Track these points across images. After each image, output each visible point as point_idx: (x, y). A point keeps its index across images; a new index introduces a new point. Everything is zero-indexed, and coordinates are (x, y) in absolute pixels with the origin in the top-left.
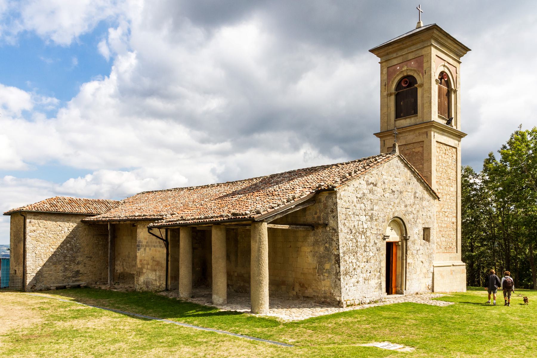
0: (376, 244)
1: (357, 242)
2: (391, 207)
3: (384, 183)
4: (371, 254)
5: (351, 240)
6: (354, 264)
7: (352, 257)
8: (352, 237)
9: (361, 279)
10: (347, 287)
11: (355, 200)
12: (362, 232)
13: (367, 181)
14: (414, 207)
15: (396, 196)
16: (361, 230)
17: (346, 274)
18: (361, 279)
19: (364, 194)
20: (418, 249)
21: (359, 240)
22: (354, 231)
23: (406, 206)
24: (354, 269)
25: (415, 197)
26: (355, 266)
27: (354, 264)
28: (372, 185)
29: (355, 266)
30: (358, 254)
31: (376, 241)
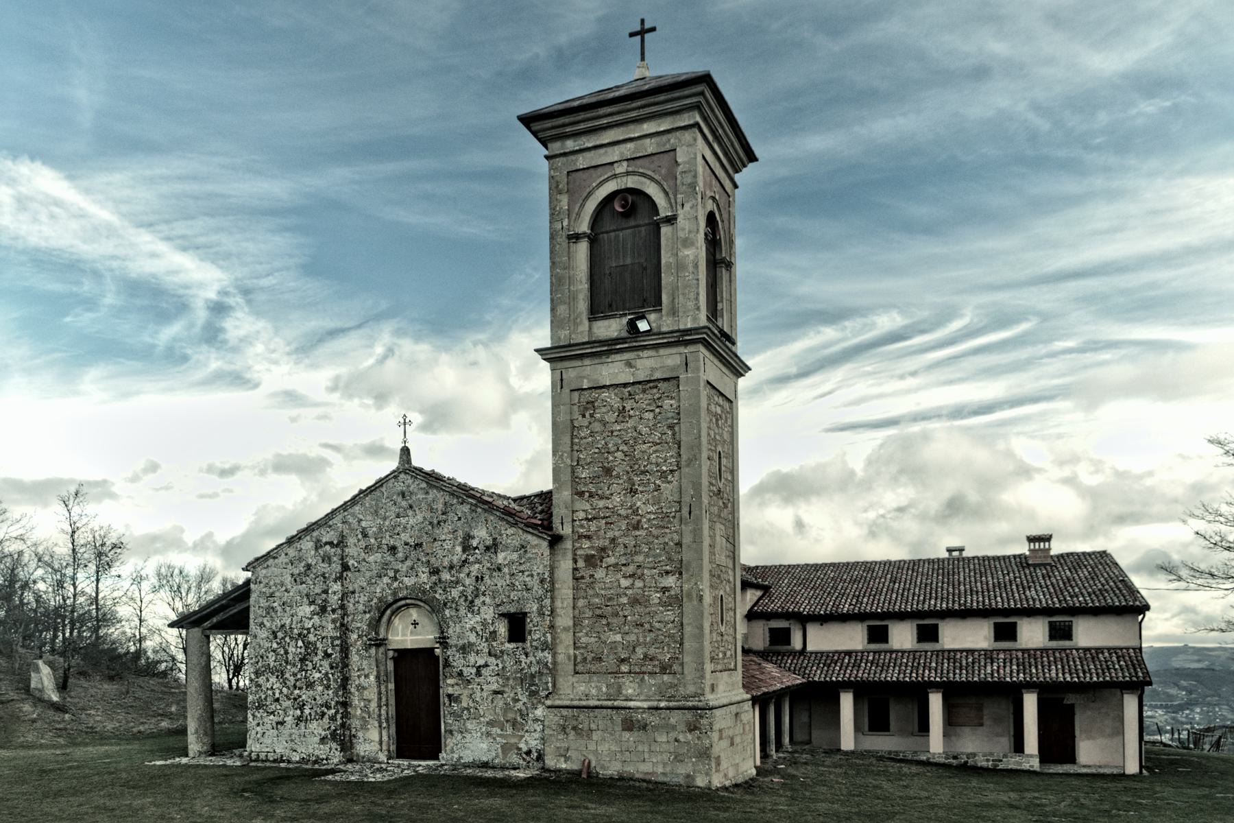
0: (327, 655)
1: (286, 653)
2: (386, 580)
3: (365, 535)
4: (317, 675)
5: (274, 651)
6: (277, 692)
7: (273, 679)
8: (275, 645)
9: (289, 719)
10: (258, 729)
11: (288, 579)
12: (299, 635)
13: (318, 541)
14: (466, 570)
15: (400, 555)
16: (296, 631)
17: (258, 708)
18: (289, 719)
19: (309, 567)
20: (481, 662)
21: (291, 649)
22: (280, 635)
23: (435, 572)
24: (277, 700)
25: (464, 551)
26: (277, 695)
27: (277, 692)
28: (328, 547)
29: (277, 695)
30: (287, 675)
31: (330, 651)
